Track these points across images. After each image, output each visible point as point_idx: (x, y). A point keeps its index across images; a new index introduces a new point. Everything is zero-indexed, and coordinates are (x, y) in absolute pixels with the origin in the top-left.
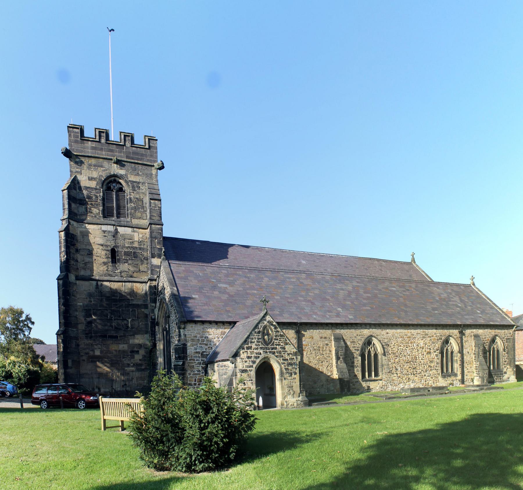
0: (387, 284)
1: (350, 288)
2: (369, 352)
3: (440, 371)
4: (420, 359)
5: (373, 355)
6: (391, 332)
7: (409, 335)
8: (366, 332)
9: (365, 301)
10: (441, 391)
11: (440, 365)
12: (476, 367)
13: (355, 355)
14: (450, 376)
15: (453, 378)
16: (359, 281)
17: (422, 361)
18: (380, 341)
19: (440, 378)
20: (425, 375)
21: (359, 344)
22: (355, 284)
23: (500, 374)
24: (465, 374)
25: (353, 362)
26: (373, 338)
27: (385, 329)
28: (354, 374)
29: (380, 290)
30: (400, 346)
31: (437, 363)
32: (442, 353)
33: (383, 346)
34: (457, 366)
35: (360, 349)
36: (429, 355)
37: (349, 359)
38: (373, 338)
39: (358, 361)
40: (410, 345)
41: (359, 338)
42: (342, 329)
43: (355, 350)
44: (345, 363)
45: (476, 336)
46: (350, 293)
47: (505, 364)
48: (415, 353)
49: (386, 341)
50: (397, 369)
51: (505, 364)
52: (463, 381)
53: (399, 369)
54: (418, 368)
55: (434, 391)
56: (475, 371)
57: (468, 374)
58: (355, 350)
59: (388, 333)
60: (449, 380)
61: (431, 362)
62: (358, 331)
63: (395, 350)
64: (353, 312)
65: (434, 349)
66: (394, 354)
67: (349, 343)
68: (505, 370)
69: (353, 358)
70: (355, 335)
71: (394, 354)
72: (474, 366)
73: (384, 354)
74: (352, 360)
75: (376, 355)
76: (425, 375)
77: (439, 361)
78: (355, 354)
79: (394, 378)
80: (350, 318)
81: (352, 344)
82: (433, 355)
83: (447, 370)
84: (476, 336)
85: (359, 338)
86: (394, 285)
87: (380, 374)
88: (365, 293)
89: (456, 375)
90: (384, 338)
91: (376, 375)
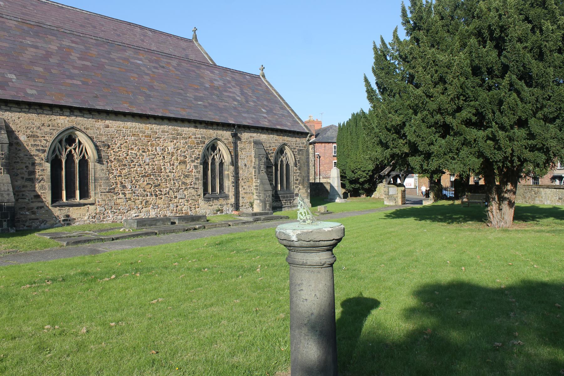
0: (129, 53)
1: (54, 47)
2: (70, 156)
3: (201, 191)
4: (168, 171)
5: (77, 161)
6: (114, 125)
7: (148, 132)
8: (64, 121)
9: (76, 72)
10: (191, 225)
11: (201, 182)
12: (256, 186)
13: (38, 161)
14: (217, 198)
15: (222, 201)
16: (78, 40)
17: (171, 175)
18: (91, 139)
19: (201, 202)
20: (176, 197)
21: (47, 140)
22: (66, 43)
23: (290, 197)
24: (241, 196)
25: (33, 173)
26: (77, 133)
27: (102, 119)
28: (33, 194)
29: (113, 60)
30: (132, 149)
31: (197, 179)
32: (205, 164)
33: (96, 146)
34: (228, 184)
35: (47, 149)
36: (183, 166)
37: (24, 166)
38: (77, 133)
39: (44, 170)
40: (150, 148)
41: (47, 129)
42: (6, 111)
43: (38, 150)
44: (8, 172)
45: (257, 143)
46: (48, 54)
47: (296, 183)
48: (159, 161)
49: (104, 139)
50: (124, 187)
51: (296, 183)
52: (237, 206)
53: (129, 186)
54: (163, 185)
55: (184, 225)
56: (255, 191)
57: (245, 196)
58: (38, 150)
59: (107, 127)
60: (216, 205)
61: (186, 176)
62: (45, 118)
63: (122, 155)
64: (40, 85)
65: (191, 157)
66: (119, 161)
67: (22, 138)
68: (296, 191)
69: (34, 164)
70: (38, 124)
71: (119, 161)
72: (254, 184)
73: (100, 160)
74: (31, 169)
75: (84, 162)
76: (176, 197)
77: (200, 176)
78: (36, 158)
79: (119, 201)
80: (31, 94)
81: (32, 140)
82: (190, 166)
83: (213, 189)
84: (257, 143)
85: (47, 129)
86: (141, 57)
87: (92, 193)
88: (80, 59)
89: (226, 197)
90: (101, 135)
91: (85, 194)
